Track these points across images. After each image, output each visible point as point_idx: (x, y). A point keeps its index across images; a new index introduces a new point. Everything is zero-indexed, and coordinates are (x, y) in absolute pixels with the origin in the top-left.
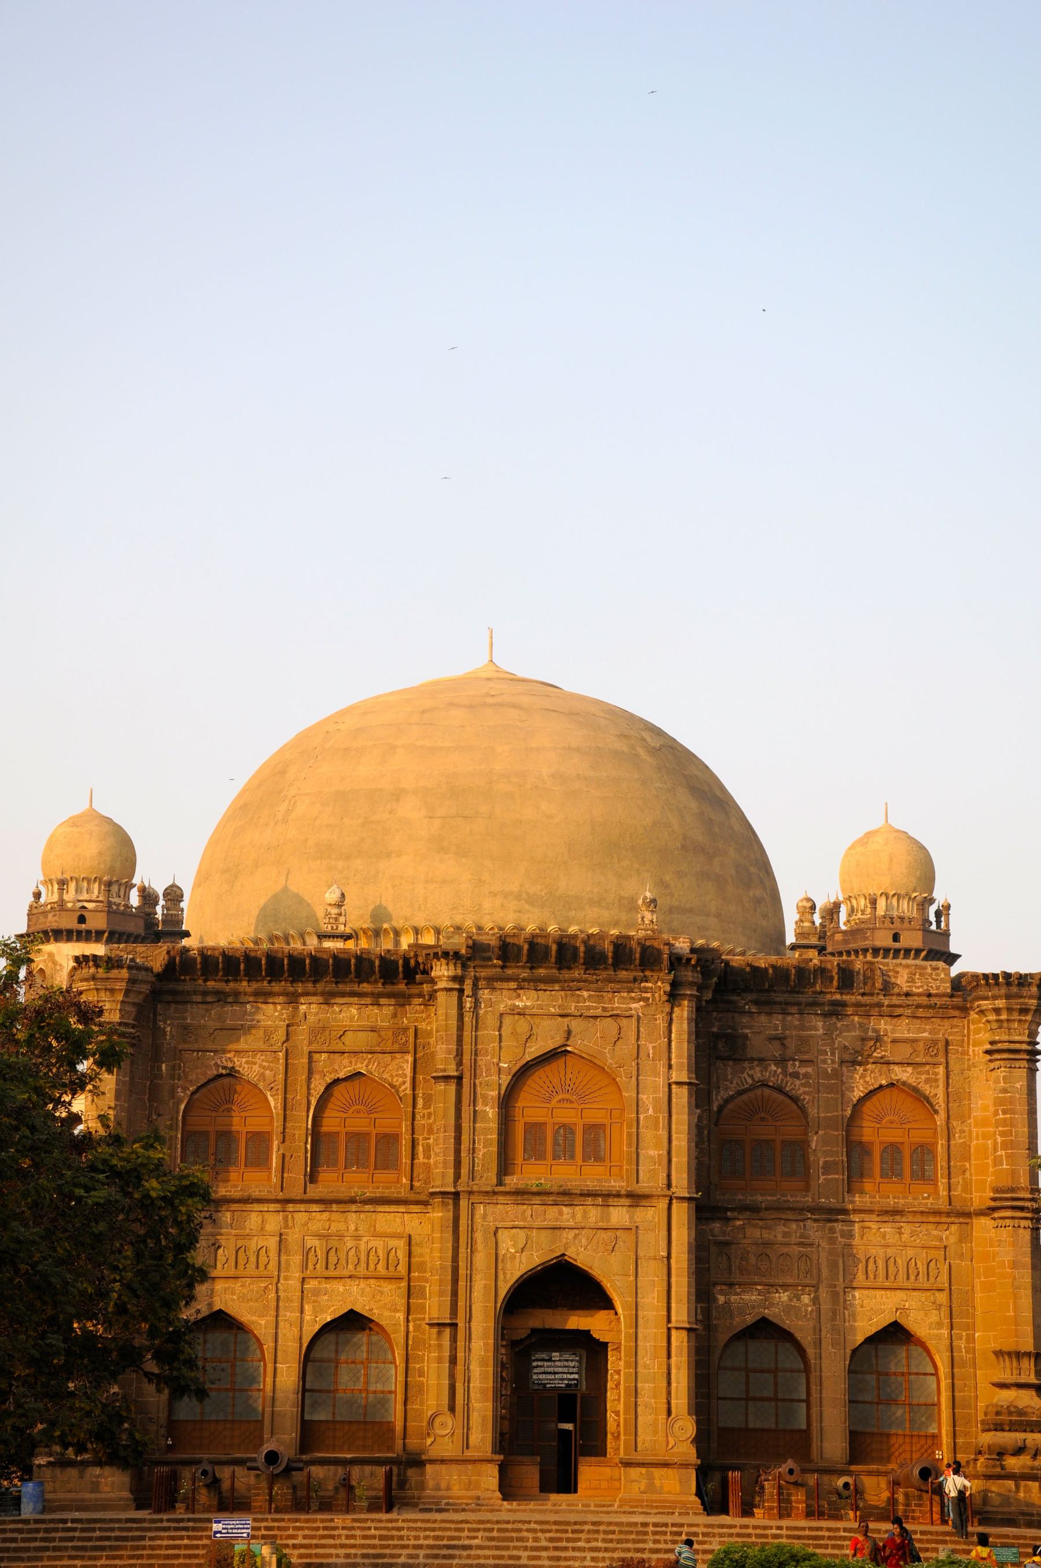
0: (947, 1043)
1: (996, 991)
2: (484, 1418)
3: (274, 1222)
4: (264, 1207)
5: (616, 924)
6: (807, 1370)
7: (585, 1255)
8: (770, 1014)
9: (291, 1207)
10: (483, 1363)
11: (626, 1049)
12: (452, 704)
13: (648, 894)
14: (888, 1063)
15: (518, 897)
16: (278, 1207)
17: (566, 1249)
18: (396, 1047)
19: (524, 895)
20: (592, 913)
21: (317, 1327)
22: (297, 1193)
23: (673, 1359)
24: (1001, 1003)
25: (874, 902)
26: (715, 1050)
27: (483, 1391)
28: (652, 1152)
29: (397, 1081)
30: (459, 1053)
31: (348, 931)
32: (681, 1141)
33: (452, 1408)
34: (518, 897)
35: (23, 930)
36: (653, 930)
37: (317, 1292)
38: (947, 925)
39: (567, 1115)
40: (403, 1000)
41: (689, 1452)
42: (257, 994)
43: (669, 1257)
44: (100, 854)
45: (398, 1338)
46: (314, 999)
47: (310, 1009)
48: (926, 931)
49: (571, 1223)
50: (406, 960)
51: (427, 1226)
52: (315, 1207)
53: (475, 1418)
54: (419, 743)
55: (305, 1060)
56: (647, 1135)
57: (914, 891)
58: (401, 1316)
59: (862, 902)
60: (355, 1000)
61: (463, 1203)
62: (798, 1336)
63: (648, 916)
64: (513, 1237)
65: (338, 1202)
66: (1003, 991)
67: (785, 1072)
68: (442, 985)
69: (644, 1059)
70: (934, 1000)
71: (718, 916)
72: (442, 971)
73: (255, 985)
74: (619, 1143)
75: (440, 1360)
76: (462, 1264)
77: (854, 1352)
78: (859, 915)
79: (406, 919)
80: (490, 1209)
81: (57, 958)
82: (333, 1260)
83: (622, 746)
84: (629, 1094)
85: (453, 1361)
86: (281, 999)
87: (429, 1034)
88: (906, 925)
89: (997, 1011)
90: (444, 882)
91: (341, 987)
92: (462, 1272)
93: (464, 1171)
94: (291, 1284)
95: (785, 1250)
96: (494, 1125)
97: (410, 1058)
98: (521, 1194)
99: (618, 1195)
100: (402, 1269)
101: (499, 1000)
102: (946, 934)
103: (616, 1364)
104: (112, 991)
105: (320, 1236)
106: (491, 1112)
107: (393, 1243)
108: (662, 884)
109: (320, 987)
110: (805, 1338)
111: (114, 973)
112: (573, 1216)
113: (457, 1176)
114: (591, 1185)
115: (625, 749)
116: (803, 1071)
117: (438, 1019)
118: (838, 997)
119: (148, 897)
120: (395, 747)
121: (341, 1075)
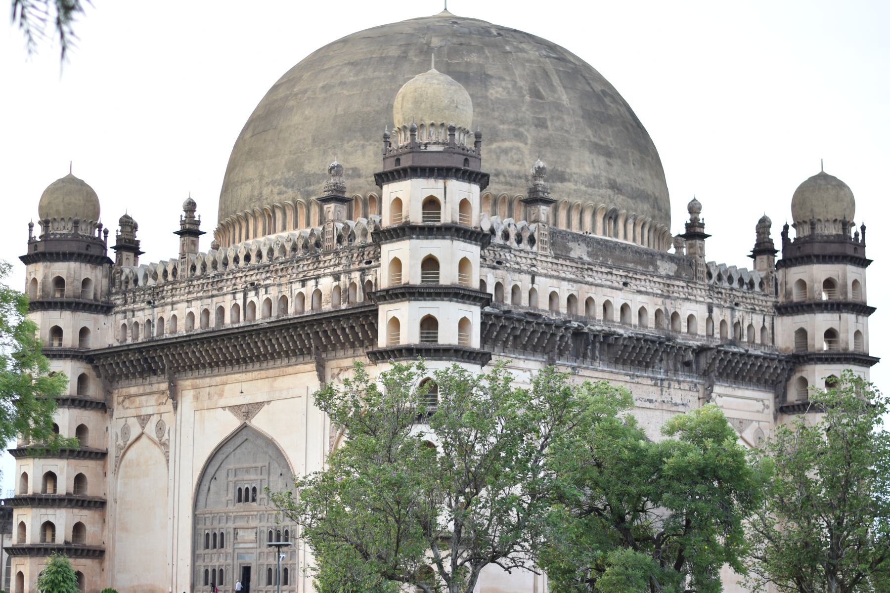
34: (279, 185)
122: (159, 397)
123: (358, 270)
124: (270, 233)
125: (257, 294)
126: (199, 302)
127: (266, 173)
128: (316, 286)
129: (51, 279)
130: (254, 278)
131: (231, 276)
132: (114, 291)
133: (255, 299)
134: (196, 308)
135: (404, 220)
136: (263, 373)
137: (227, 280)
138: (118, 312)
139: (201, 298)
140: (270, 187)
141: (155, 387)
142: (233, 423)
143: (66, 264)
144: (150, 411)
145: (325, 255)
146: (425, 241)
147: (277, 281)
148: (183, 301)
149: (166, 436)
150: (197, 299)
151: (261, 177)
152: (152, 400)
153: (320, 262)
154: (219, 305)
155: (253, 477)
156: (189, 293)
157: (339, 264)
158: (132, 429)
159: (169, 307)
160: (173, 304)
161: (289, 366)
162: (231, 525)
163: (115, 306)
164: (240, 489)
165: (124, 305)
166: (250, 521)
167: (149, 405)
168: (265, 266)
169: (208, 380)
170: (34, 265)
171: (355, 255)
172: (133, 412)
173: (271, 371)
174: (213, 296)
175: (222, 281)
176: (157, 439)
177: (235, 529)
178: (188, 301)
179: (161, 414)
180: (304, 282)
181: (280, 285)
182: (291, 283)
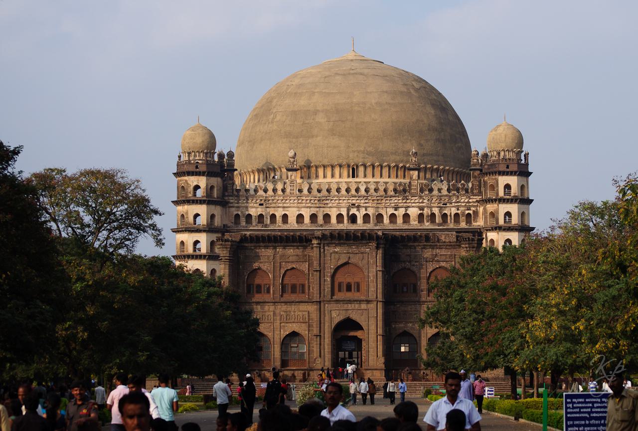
0: (455, 255)
1: (466, 242)
2: (329, 359)
3: (272, 308)
4: (269, 304)
5: (402, 162)
6: (417, 344)
7: (355, 316)
8: (406, 249)
9: (276, 304)
10: (328, 345)
11: (365, 261)
12: (337, 74)
13: (414, 150)
14: (439, 261)
15: (363, 152)
16: (273, 304)
17: (350, 315)
18: (303, 260)
19: (366, 152)
20: (393, 157)
21: (285, 335)
22: (278, 300)
23: (378, 343)
24: (467, 246)
25: (499, 154)
26: (389, 261)
27: (328, 352)
28: (372, 289)
29: (304, 270)
30: (320, 264)
31: (298, 167)
32: (380, 286)
33: (320, 356)
34: (363, 152)
35: (175, 172)
36: (416, 165)
37: (284, 326)
38: (528, 161)
39: (349, 280)
40: (305, 247)
41: (383, 366)
42: (265, 246)
43: (377, 317)
44: (203, 141)
45: (306, 338)
46: (281, 247)
47: (279, 250)
48: (519, 164)
49: (351, 308)
50: (305, 236)
51: (313, 308)
52: (283, 304)
53: (326, 359)
54: (324, 91)
55: (279, 264)
56: (371, 284)
57: (515, 148)
58: (307, 332)
59: (495, 153)
60: (292, 247)
61: (322, 304)
62: (414, 335)
63: (414, 159)
64: (335, 312)
65: (289, 302)
66: (468, 242)
67: (410, 265)
68: (315, 245)
69: (371, 266)
70: (452, 244)
71: (443, 156)
72: (315, 242)
73: (264, 244)
74: (363, 287)
75: (317, 344)
76: (322, 320)
77: (429, 339)
78: (494, 158)
79: (320, 162)
80: (329, 305)
81: (189, 182)
82: (288, 318)
83: (404, 89)
84: (366, 274)
85: (320, 344)
86: (272, 248)
87: (312, 256)
88: (511, 162)
89: (466, 248)
90: (334, 147)
91: (288, 244)
92: (322, 321)
93: (322, 295)
94: (277, 324)
95: (411, 312)
96: (330, 283)
97: (307, 263)
98: (337, 301)
99: (363, 301)
100: (307, 320)
101: (330, 249)
102: (527, 165)
103: (364, 344)
104: (227, 248)
105: (285, 312)
106: (329, 279)
107: (304, 313)
108: (420, 145)
109: (282, 244)
110: (416, 335)
111: (227, 243)
112: (351, 306)
113: (320, 297)
114: (356, 298)
115: (406, 90)
116: (416, 264)
117: (314, 253)
118: (425, 243)
119: (221, 156)
120: (314, 93)
121: (289, 268)
123: (437, 207)
124: (353, 177)
125: (358, 210)
126: (308, 209)
128: (406, 211)
129: (209, 187)
132: (227, 194)
133: (357, 213)
135: (512, 195)
138: (233, 207)
140: (356, 154)
143: (216, 178)
146: (522, 205)
147: (375, 205)
148: (294, 207)
153: (408, 199)
154: (325, 213)
156: (298, 203)
157: (422, 202)
159: (281, 209)
160: (284, 207)
163: (228, 203)
165: (238, 203)
168: (364, 196)
170: (197, 177)
171: (435, 199)
174: (321, 207)
180: (396, 209)
181: (378, 208)
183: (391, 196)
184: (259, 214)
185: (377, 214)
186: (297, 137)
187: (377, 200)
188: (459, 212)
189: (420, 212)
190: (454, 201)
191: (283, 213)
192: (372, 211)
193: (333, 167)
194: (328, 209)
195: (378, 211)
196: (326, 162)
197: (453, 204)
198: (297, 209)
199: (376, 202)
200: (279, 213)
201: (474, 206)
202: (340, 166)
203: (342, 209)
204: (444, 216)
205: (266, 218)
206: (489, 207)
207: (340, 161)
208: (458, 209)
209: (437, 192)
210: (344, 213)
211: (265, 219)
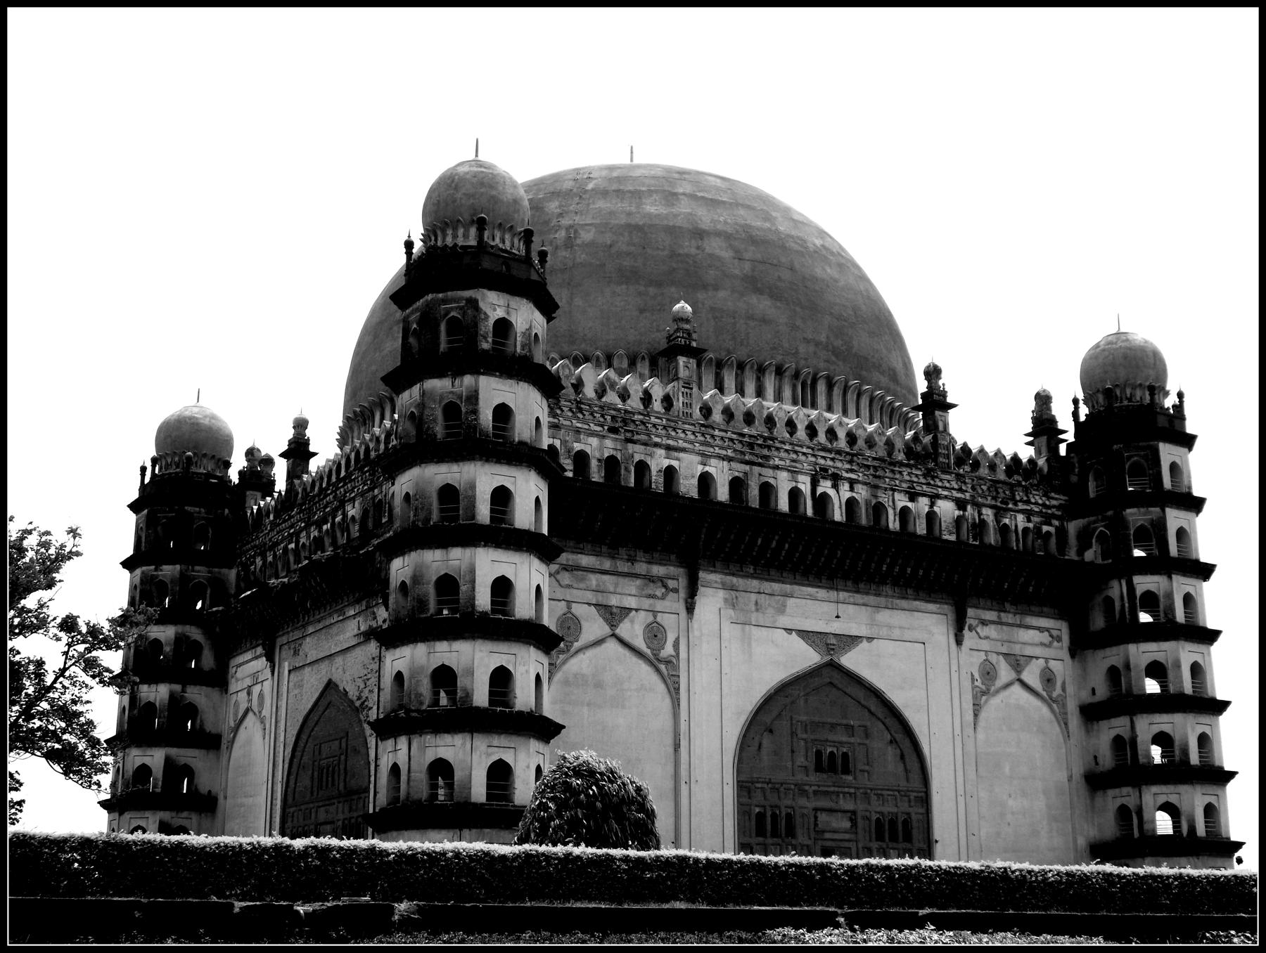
79: (729, 352)
122: (646, 585)
123: (991, 507)
125: (835, 486)
127: (799, 322)
128: (932, 505)
130: (822, 461)
131: (787, 447)
133: (832, 492)
134: (722, 474)
136: (859, 598)
137: (778, 449)
139: (730, 459)
140: (812, 349)
141: (641, 568)
142: (809, 657)
144: (631, 602)
145: (944, 472)
149: (668, 650)
150: (723, 458)
151: (794, 328)
152: (632, 586)
153: (933, 478)
155: (844, 739)
156: (702, 444)
157: (960, 490)
158: (585, 625)
159: (662, 452)
160: (668, 448)
161: (903, 598)
162: (807, 804)
164: (819, 754)
166: (841, 802)
167: (626, 594)
168: (848, 453)
169: (754, 584)
170: (507, 296)
172: (590, 597)
173: (872, 598)
175: (769, 447)
176: (648, 652)
177: (816, 810)
178: (703, 455)
179: (655, 613)
180: (913, 497)
181: (876, 487)
182: (894, 490)
183: (901, 464)
184: (606, 455)
185: (874, 502)
186: (659, 284)
187: (875, 467)
188: (1031, 525)
189: (957, 513)
190: (1018, 498)
191: (666, 463)
192: (864, 493)
193: (761, 370)
194: (770, 472)
195: (876, 497)
196: (741, 354)
197: (1021, 506)
198: (699, 458)
199: (872, 471)
200: (659, 461)
201: (1057, 517)
202: (779, 372)
203: (801, 478)
204: (1004, 530)
205: (626, 469)
206: (1132, 514)
207: (779, 358)
208: (1029, 521)
209: (987, 471)
210: (805, 485)
211: (623, 472)
